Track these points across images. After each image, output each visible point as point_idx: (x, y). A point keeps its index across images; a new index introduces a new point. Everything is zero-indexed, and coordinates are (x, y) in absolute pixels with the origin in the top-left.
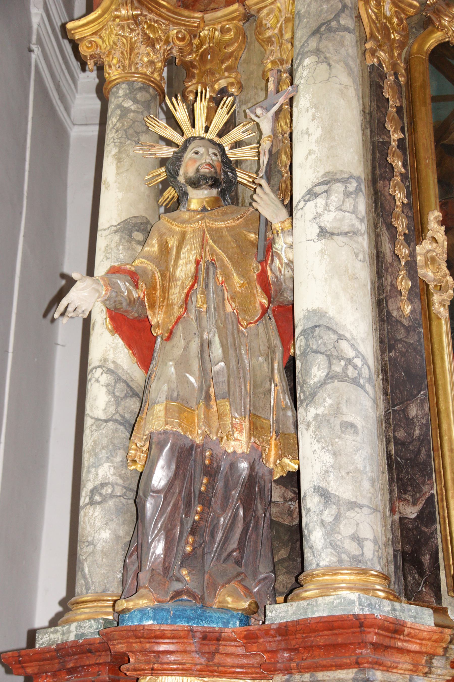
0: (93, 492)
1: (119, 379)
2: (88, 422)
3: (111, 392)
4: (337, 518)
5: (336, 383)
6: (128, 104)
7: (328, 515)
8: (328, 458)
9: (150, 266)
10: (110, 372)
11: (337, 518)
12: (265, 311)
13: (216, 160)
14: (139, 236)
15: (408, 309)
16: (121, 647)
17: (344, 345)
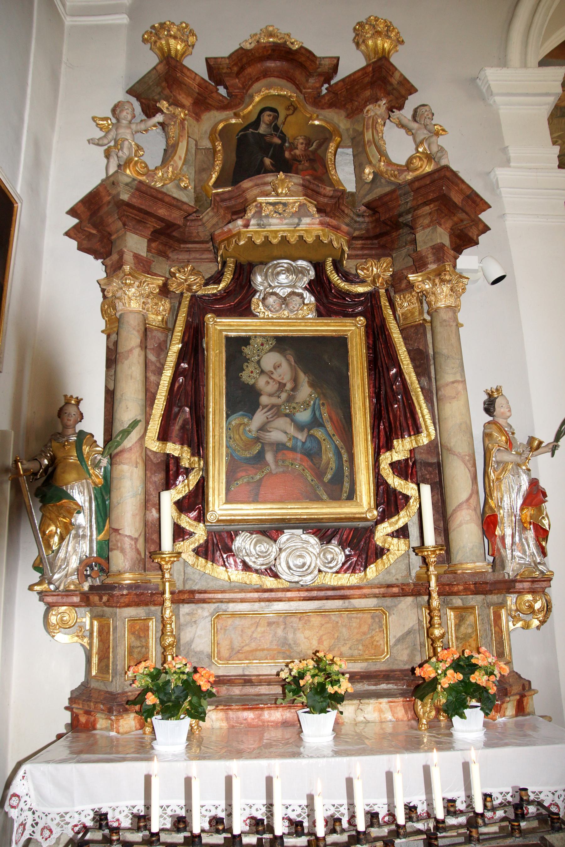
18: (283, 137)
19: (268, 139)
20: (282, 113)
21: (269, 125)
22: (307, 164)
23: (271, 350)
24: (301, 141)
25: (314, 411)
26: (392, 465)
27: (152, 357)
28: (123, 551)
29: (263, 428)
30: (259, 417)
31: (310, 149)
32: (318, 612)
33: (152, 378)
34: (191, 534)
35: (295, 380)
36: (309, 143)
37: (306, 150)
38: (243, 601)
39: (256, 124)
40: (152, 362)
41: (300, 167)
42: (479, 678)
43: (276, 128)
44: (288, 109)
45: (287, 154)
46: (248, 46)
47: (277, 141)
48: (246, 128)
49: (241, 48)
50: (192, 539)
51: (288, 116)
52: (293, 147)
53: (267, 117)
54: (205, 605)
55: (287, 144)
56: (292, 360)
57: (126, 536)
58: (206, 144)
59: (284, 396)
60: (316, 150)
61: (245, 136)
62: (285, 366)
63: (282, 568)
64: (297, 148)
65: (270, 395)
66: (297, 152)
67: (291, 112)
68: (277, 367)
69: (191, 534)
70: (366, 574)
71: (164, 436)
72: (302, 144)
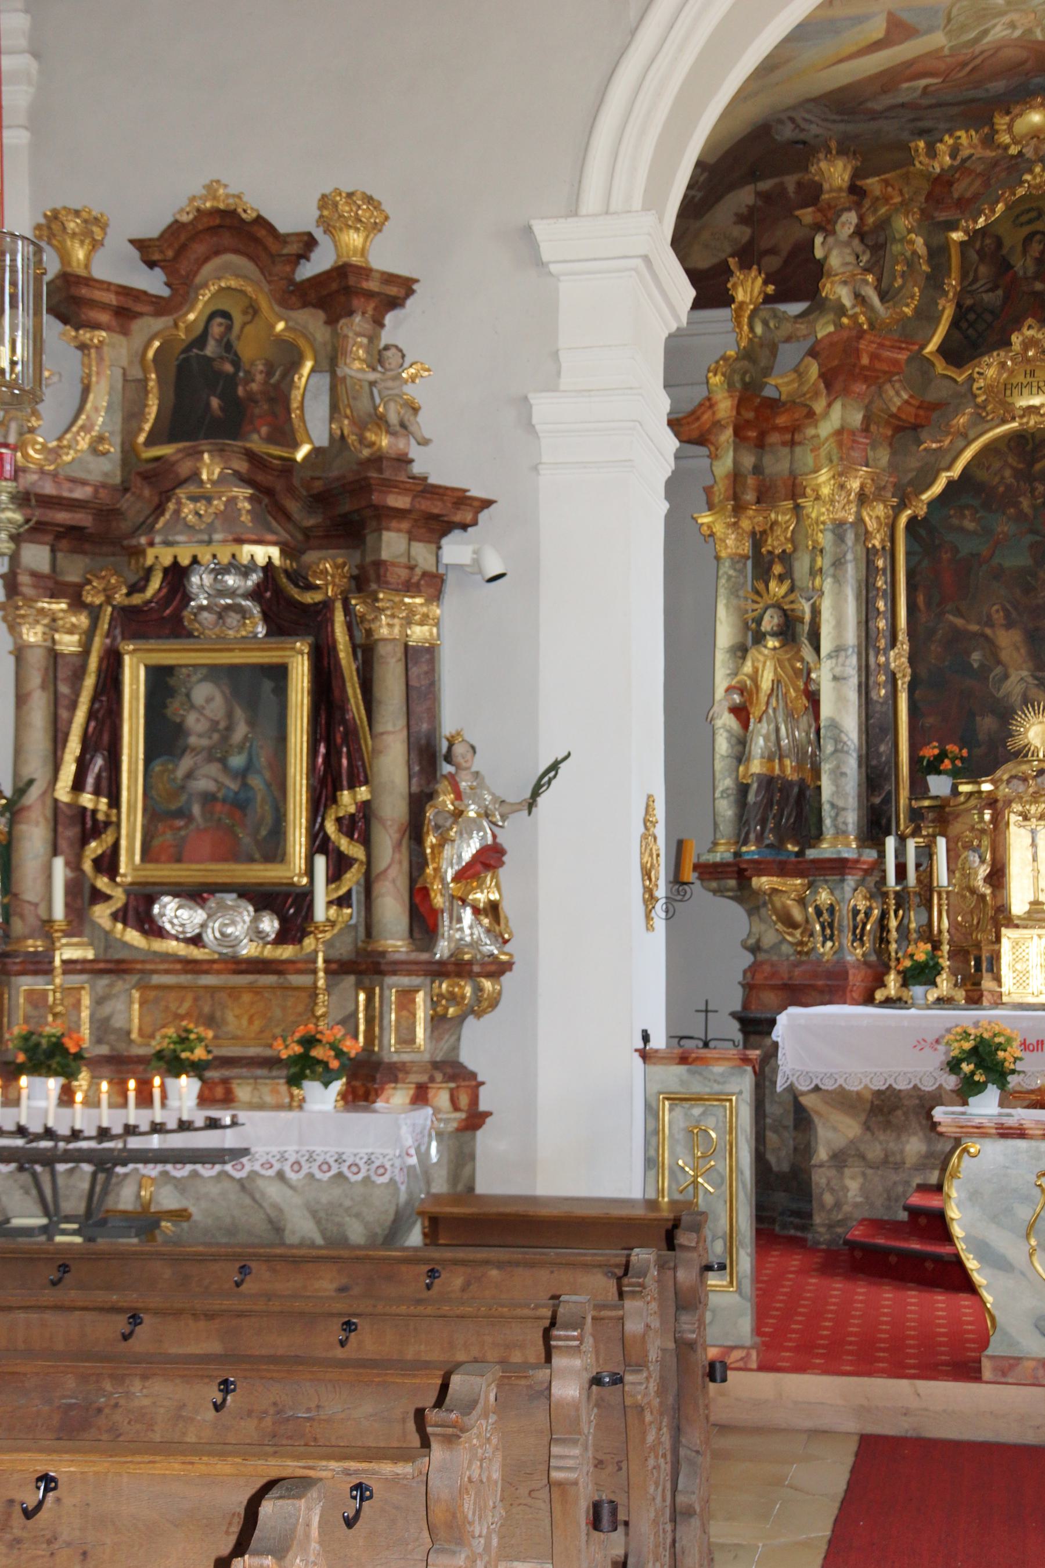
0: (722, 792)
1: (732, 735)
2: (717, 756)
3: (729, 742)
4: (837, 815)
5: (839, 754)
6: (731, 572)
7: (833, 813)
8: (834, 788)
9: (748, 682)
10: (728, 731)
11: (837, 815)
12: (806, 708)
13: (782, 620)
14: (739, 654)
15: (883, 692)
16: (744, 866)
17: (843, 736)
18: (237, 363)
19: (217, 365)
20: (238, 319)
21: (219, 341)
22: (266, 407)
23: (201, 681)
24: (261, 367)
25: (250, 755)
26: (339, 820)
27: (64, 689)
28: (22, 917)
29: (190, 775)
30: (186, 763)
31: (273, 381)
32: (252, 989)
33: (64, 714)
34: (107, 898)
35: (230, 715)
36: (269, 373)
37: (266, 382)
38: (167, 972)
39: (201, 341)
40: (64, 696)
41: (257, 411)
42: (317, 1053)
43: (228, 347)
44: (245, 313)
45: (241, 391)
46: (185, 218)
47: (229, 368)
48: (188, 349)
49: (176, 221)
50: (111, 902)
51: (244, 325)
52: (250, 378)
53: (216, 330)
54: (127, 977)
55: (241, 374)
56: (227, 692)
57: (29, 902)
58: (136, 373)
59: (216, 736)
60: (279, 382)
61: (186, 360)
62: (219, 701)
63: (209, 937)
64: (253, 381)
65: (200, 736)
66: (254, 386)
67: (249, 317)
68: (209, 700)
69: (107, 898)
70: (302, 948)
71: (78, 786)
72: (261, 372)
